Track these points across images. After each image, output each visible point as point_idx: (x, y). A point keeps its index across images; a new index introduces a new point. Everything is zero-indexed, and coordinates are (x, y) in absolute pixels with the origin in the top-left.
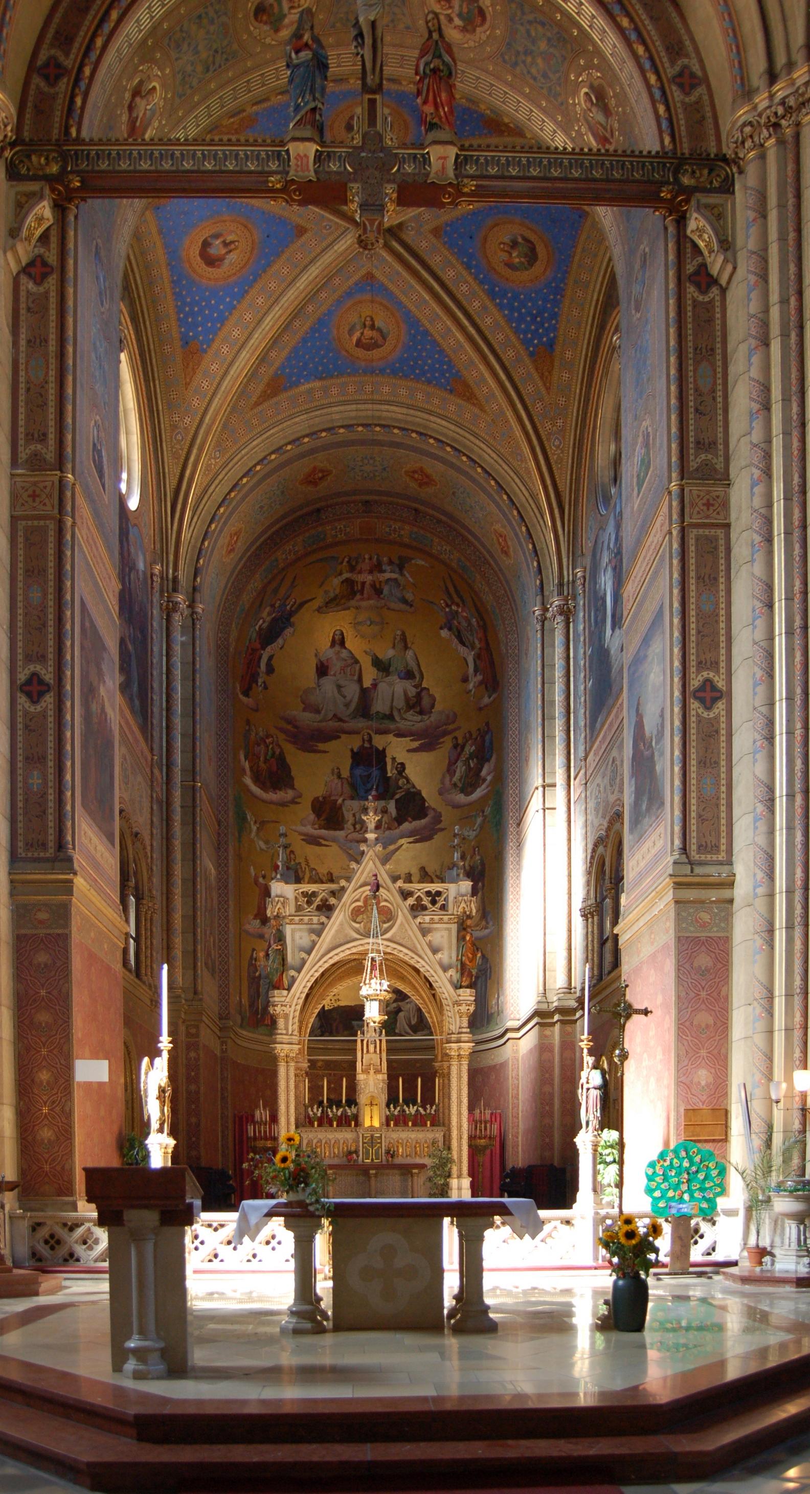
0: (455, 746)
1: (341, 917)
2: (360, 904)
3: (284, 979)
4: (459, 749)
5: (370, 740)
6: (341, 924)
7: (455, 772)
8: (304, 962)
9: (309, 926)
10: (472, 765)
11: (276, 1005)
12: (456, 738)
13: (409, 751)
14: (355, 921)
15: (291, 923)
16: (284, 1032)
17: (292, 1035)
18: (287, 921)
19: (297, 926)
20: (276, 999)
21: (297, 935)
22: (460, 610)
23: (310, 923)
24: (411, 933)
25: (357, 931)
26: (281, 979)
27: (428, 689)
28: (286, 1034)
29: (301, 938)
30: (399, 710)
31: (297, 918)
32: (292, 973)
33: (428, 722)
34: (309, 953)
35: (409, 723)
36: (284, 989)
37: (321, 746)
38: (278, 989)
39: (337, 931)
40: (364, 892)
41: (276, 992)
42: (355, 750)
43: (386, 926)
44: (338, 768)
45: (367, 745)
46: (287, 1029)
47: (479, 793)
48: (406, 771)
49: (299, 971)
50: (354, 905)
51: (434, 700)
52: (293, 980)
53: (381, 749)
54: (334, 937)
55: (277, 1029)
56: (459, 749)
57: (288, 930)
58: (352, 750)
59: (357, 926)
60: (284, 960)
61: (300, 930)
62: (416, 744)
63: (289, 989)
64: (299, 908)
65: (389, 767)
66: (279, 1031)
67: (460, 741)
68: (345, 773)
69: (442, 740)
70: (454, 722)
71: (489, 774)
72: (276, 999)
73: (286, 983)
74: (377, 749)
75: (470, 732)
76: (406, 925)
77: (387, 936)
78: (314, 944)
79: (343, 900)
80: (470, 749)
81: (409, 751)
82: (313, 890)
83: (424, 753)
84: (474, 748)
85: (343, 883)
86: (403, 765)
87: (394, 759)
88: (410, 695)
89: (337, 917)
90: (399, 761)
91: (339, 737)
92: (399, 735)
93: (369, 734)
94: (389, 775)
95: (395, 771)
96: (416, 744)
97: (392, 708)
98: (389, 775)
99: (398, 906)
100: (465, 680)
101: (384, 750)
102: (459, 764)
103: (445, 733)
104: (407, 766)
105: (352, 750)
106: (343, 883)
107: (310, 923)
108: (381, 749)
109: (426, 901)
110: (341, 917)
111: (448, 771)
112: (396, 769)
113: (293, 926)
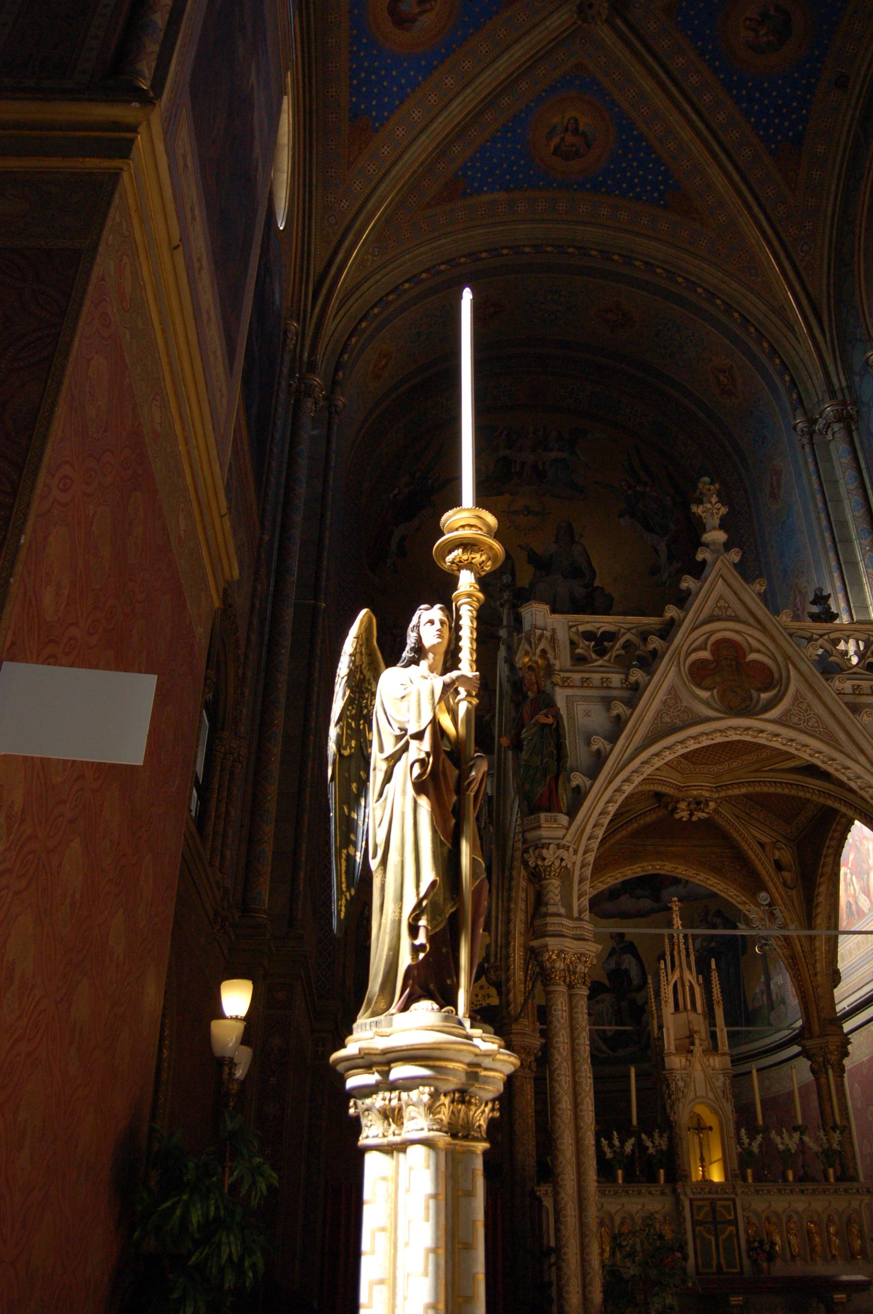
1: (671, 675)
2: (705, 655)
3: (561, 791)
6: (672, 690)
8: (600, 759)
9: (602, 693)
11: (547, 846)
14: (699, 685)
15: (566, 683)
16: (562, 911)
17: (579, 919)
18: (557, 679)
19: (578, 692)
20: (544, 833)
21: (580, 709)
23: (605, 685)
24: (820, 710)
25: (707, 704)
26: (553, 791)
28: (570, 916)
29: (587, 714)
31: (576, 677)
32: (577, 779)
34: (613, 738)
36: (560, 811)
38: (549, 810)
39: (665, 702)
40: (712, 633)
41: (543, 816)
43: (764, 696)
46: (569, 907)
49: (593, 774)
50: (694, 656)
52: (579, 795)
54: (659, 715)
55: (547, 904)
57: (560, 697)
59: (705, 694)
60: (560, 747)
61: (585, 699)
63: (572, 813)
64: (579, 660)
66: (552, 909)
72: (544, 833)
73: (564, 798)
76: (810, 697)
77: (774, 713)
78: (619, 723)
79: (676, 641)
82: (607, 628)
85: (671, 611)
89: (665, 676)
99: (787, 658)
100: (655, 571)
106: (671, 611)
107: (605, 685)
110: (671, 675)
113: (569, 692)
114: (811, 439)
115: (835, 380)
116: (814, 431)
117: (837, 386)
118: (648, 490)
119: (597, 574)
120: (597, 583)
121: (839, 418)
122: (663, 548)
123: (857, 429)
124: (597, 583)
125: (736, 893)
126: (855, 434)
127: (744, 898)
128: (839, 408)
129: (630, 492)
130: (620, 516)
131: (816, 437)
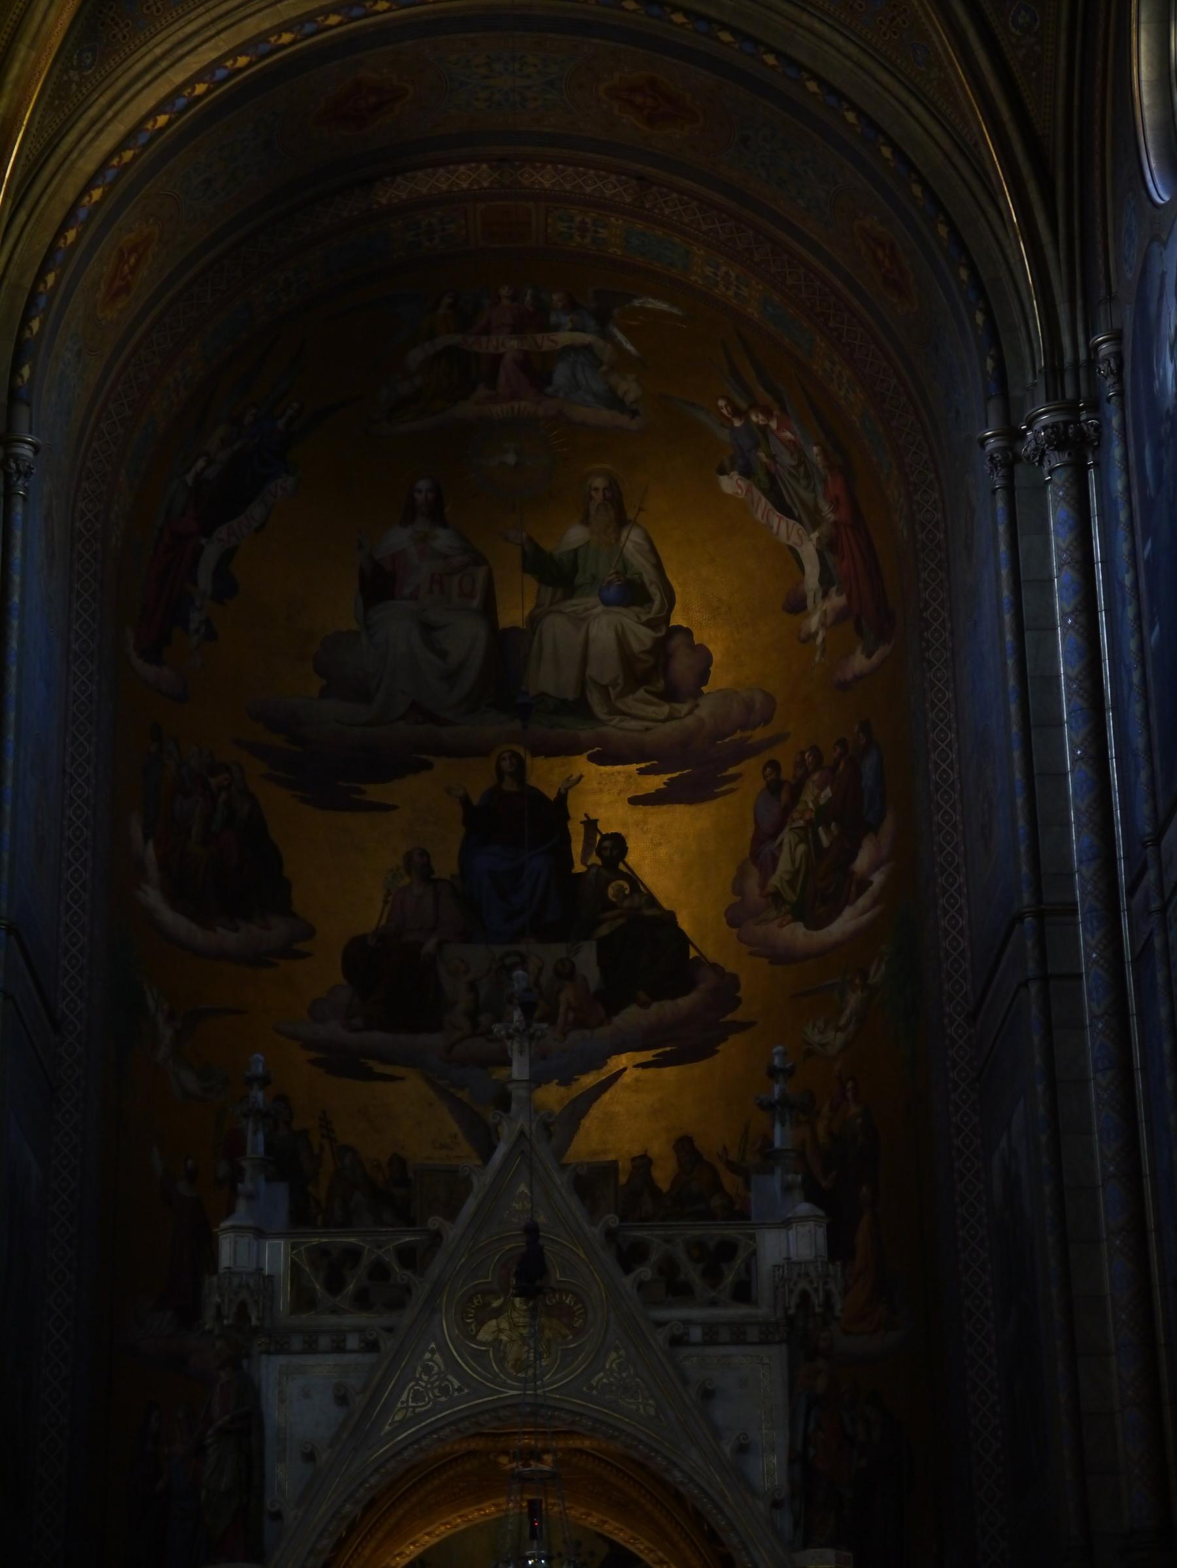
0: (774, 787)
4: (784, 795)
5: (520, 770)
7: (775, 860)
10: (825, 841)
12: (774, 765)
13: (634, 801)
22: (774, 425)
27: (688, 632)
30: (604, 690)
33: (690, 721)
35: (633, 724)
37: (374, 792)
42: (475, 801)
44: (424, 854)
45: (509, 786)
47: (845, 923)
48: (632, 858)
51: (708, 658)
53: (552, 795)
56: (784, 795)
58: (466, 802)
62: (656, 782)
65: (577, 848)
67: (788, 772)
68: (446, 865)
69: (732, 771)
70: (767, 720)
71: (875, 867)
74: (540, 797)
75: (816, 751)
80: (816, 795)
81: (634, 801)
83: (680, 809)
84: (828, 792)
86: (618, 844)
87: (591, 825)
88: (636, 647)
90: (605, 828)
91: (429, 766)
92: (600, 759)
93: (515, 755)
94: (579, 868)
95: (595, 859)
96: (656, 782)
97: (582, 683)
98: (579, 868)
101: (562, 798)
102: (787, 837)
103: (743, 753)
104: (630, 844)
105: (466, 802)
108: (552, 795)
109: (692, 1273)
111: (755, 856)
112: (599, 854)
114: (1010, 478)
115: (1066, 340)
116: (1017, 458)
117: (1068, 357)
118: (774, 425)
119: (678, 598)
120: (677, 619)
121: (1059, 439)
122: (809, 553)
123: (1097, 465)
124: (677, 619)
125: (650, 1546)
126: (1092, 474)
127: (660, 1554)
128: (1059, 418)
129: (737, 423)
130: (722, 471)
131: (1019, 470)
